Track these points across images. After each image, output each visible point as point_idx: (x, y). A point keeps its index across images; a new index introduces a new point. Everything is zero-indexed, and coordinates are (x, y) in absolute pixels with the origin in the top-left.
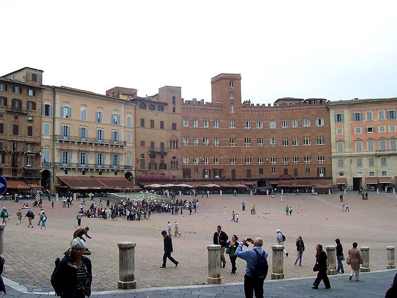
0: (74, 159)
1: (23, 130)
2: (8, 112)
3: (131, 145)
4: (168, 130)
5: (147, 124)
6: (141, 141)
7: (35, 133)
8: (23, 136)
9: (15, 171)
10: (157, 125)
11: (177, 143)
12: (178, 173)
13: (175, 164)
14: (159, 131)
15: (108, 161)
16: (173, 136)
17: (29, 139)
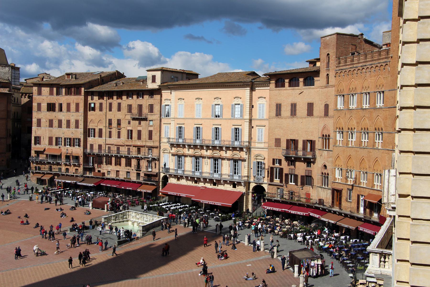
0: (188, 165)
1: (145, 135)
2: (134, 119)
3: (262, 145)
4: (320, 117)
5: (286, 111)
6: (276, 139)
7: (155, 137)
8: (145, 141)
9: (138, 175)
10: (302, 110)
11: (329, 139)
12: (326, 196)
13: (325, 177)
14: (304, 120)
15: (226, 168)
16: (324, 128)
17: (150, 143)
